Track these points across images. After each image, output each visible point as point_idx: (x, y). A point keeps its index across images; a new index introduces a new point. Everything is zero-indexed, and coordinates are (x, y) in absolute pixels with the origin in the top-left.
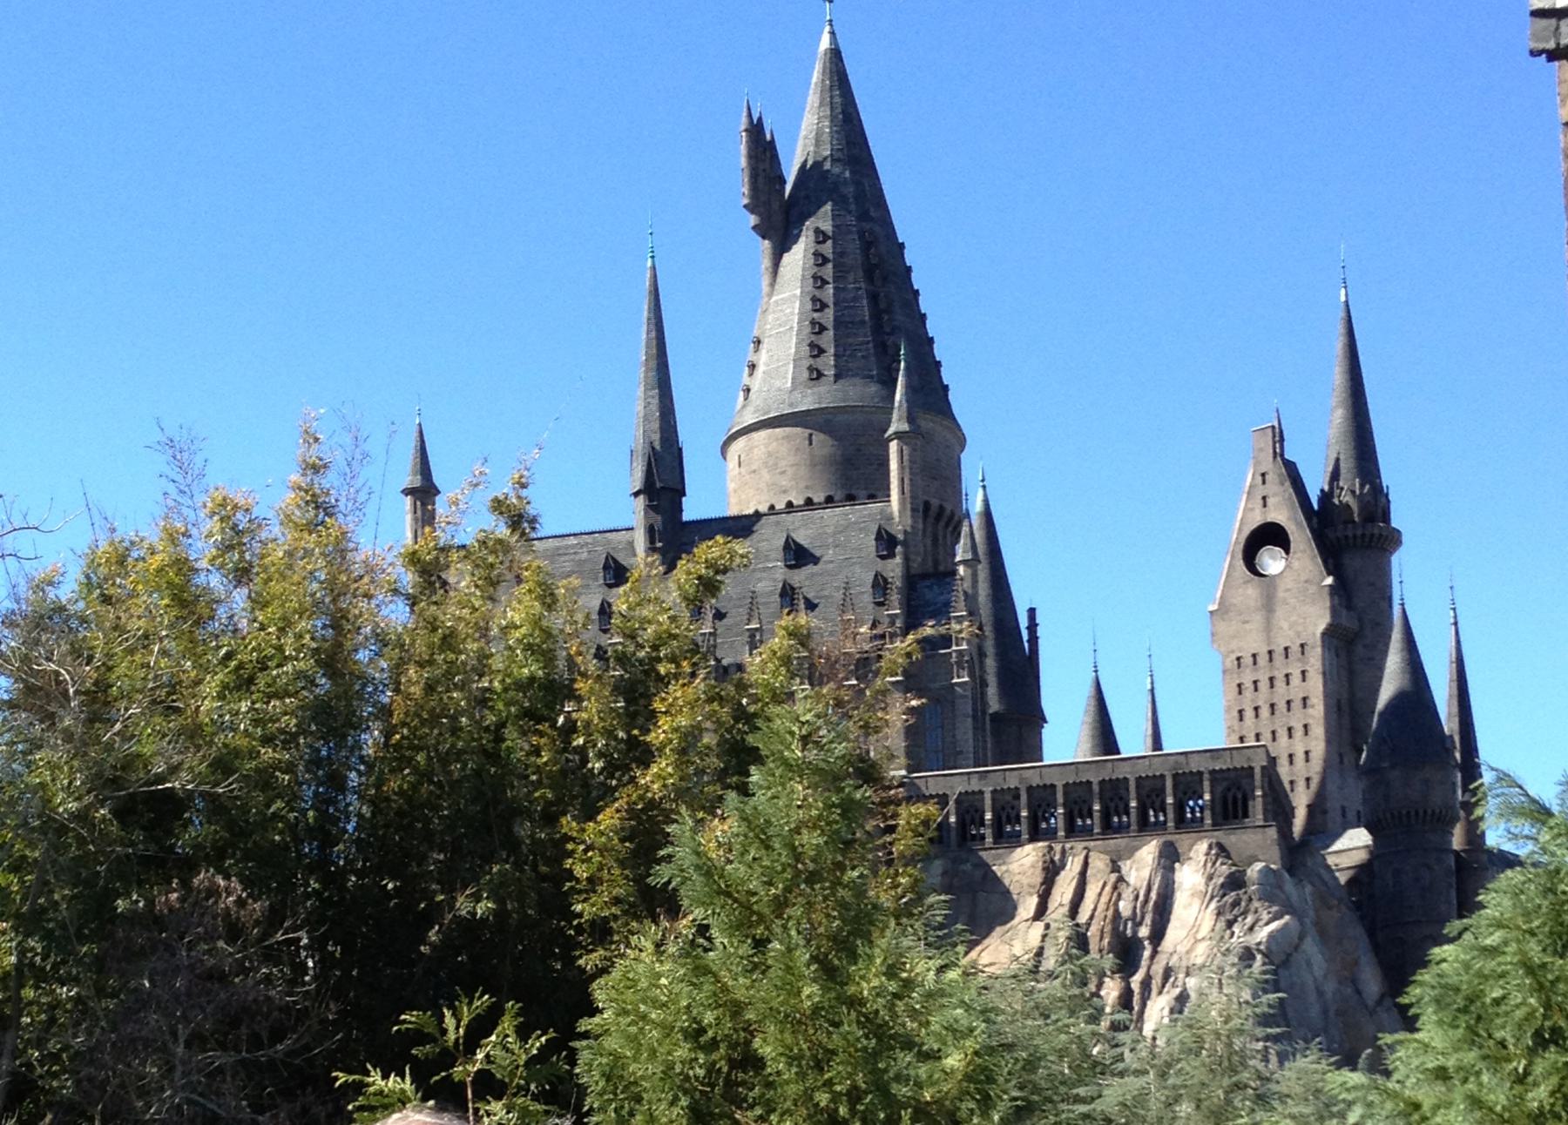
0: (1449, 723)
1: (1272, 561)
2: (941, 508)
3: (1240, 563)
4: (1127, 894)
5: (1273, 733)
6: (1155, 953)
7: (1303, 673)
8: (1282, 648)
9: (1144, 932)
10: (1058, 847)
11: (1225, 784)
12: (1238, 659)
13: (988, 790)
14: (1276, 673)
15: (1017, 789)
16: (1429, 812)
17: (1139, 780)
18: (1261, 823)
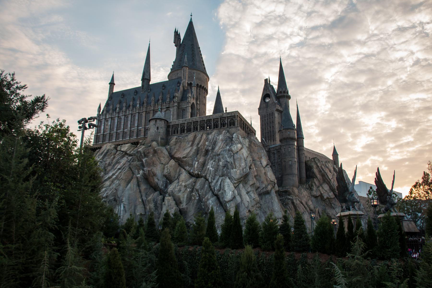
0: (295, 122)
2: (201, 85)
3: (263, 101)
6: (212, 152)
9: (210, 148)
10: (197, 133)
11: (230, 119)
13: (186, 123)
17: (214, 119)
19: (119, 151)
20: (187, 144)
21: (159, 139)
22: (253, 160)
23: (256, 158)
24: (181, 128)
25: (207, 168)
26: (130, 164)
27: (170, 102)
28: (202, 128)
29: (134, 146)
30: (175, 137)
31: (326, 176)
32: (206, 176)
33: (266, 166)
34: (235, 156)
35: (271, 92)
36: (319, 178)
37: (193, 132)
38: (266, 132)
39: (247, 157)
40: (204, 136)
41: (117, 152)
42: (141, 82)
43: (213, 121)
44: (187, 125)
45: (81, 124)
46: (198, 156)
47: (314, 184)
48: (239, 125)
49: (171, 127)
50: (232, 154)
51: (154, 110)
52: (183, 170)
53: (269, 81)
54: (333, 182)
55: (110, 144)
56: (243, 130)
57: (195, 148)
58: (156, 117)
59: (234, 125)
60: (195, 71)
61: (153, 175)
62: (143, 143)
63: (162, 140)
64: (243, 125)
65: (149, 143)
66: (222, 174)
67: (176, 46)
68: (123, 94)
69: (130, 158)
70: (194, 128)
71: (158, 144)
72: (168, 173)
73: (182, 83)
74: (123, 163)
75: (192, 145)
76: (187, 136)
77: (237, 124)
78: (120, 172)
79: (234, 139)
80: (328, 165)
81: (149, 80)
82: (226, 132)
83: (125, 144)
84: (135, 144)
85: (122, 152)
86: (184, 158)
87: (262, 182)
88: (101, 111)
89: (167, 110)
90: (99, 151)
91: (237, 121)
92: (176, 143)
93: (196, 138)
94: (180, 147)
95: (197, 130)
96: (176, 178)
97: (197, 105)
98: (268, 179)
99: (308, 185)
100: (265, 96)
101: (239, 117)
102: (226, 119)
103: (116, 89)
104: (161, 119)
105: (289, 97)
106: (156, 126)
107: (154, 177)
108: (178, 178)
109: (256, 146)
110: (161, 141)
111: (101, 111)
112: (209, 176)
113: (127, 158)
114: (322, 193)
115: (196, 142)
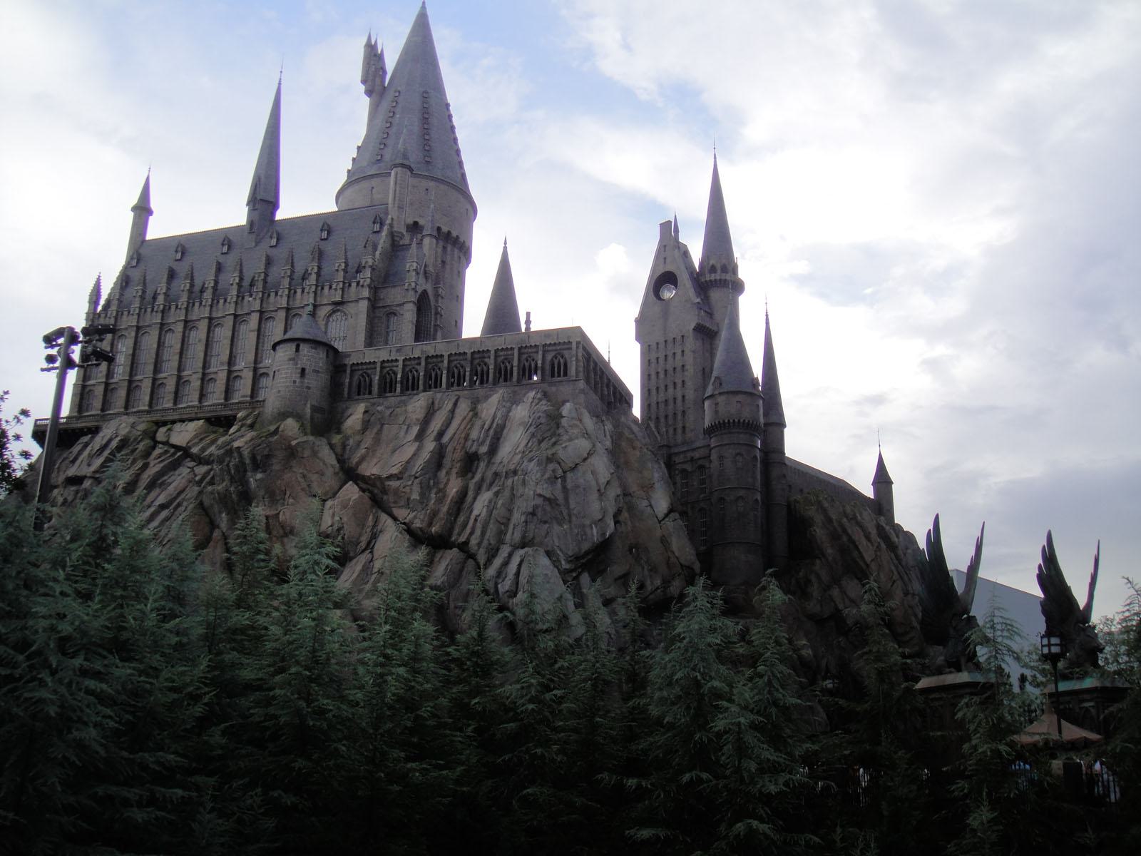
0: (757, 370)
1: (668, 294)
2: (449, 233)
4: (478, 423)
5: (666, 386)
6: (489, 463)
7: (683, 351)
8: (671, 339)
9: (484, 449)
10: (439, 395)
12: (649, 346)
13: (401, 359)
14: (668, 353)
15: (419, 358)
17: (496, 351)
18: (574, 378)
19: (163, 443)
20: (402, 433)
21: (308, 411)
22: (625, 495)
23: (634, 488)
24: (382, 378)
25: (473, 517)
26: (201, 493)
27: (347, 284)
28: (456, 380)
29: (215, 429)
30: (361, 407)
31: (855, 554)
32: (466, 543)
33: (667, 515)
34: (569, 481)
35: (683, 268)
36: (830, 559)
37: (425, 391)
38: (660, 400)
39: (608, 482)
40: (464, 407)
41: (154, 448)
42: (245, 210)
43: (496, 357)
44: (404, 366)
45: (52, 347)
46: (442, 474)
47: (813, 578)
48: (581, 375)
49: (348, 371)
50: (560, 472)
51: (288, 309)
52: (390, 521)
53: (677, 231)
55: (131, 419)
56: (595, 391)
57: (430, 445)
58: (298, 335)
59: (565, 374)
60: (432, 184)
61: (281, 532)
62: (249, 422)
63: (317, 415)
64: (595, 373)
65: (271, 423)
66: (524, 537)
67: (369, 93)
68: (182, 246)
69: (202, 470)
70: (428, 376)
71: (302, 425)
72: (336, 527)
73: (388, 222)
74: (176, 488)
75: (420, 437)
76: (405, 403)
77: (577, 372)
78: (167, 519)
79: (564, 422)
80: (861, 514)
81: (274, 205)
82: (539, 396)
83: (183, 421)
84: (221, 422)
85: (172, 450)
86: (390, 477)
87: (654, 570)
88: (102, 302)
89: (334, 312)
90: (92, 438)
91: (577, 360)
92: (366, 425)
93: (435, 411)
94: (377, 440)
95: (437, 384)
96: (363, 545)
97: (437, 301)
98: (673, 559)
100: (662, 280)
101: (584, 349)
102: (540, 353)
103: (155, 231)
104: (316, 343)
105: (738, 287)
106: (297, 364)
107: (286, 540)
108: (370, 546)
109: (634, 448)
110: (312, 418)
111: (102, 302)
112: (479, 545)
113: (192, 468)
114: (841, 606)
115: (436, 425)
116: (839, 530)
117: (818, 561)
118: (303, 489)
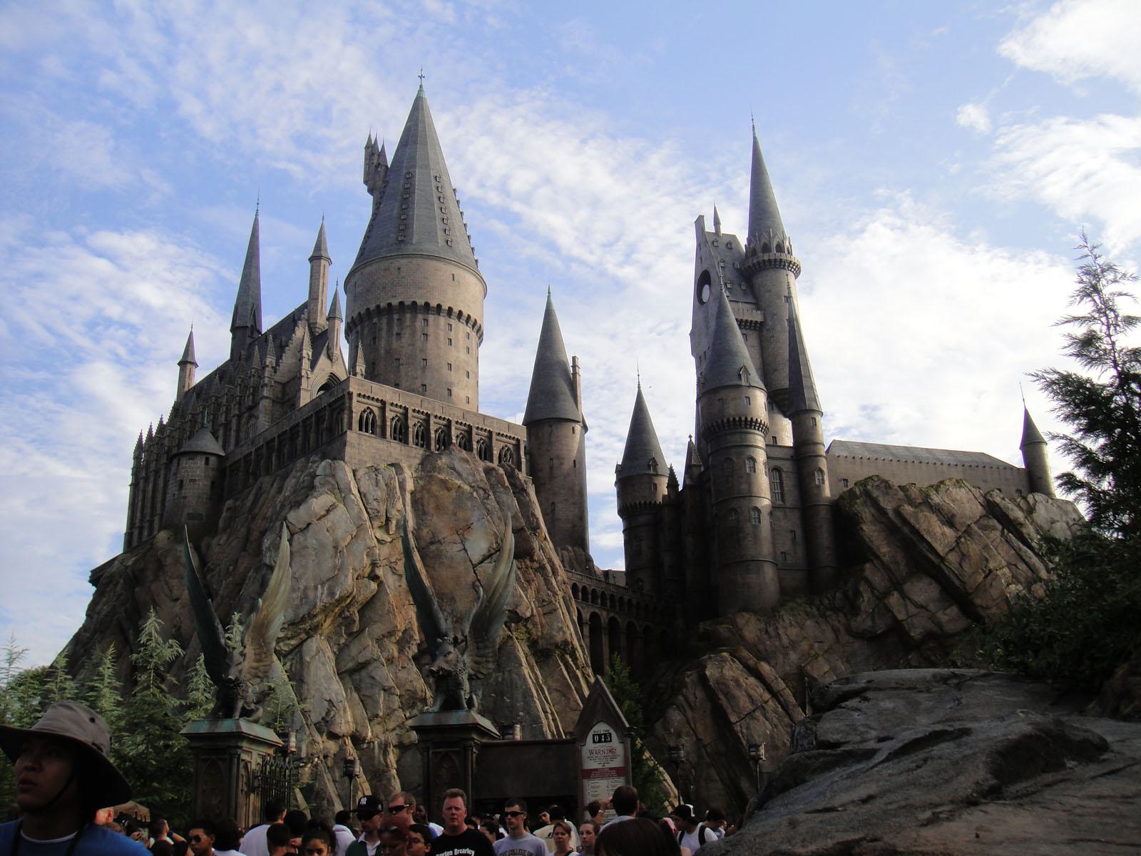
2: (427, 304)
13: (253, 450)
16: (725, 420)
36: (886, 559)
47: (863, 587)
53: (717, 223)
54: (955, 566)
67: (371, 191)
79: (317, 481)
81: (255, 328)
89: (251, 416)
99: (838, 595)
100: (703, 279)
109: (449, 490)
114: (901, 616)
116: (898, 522)
117: (868, 566)
118: (166, 596)
